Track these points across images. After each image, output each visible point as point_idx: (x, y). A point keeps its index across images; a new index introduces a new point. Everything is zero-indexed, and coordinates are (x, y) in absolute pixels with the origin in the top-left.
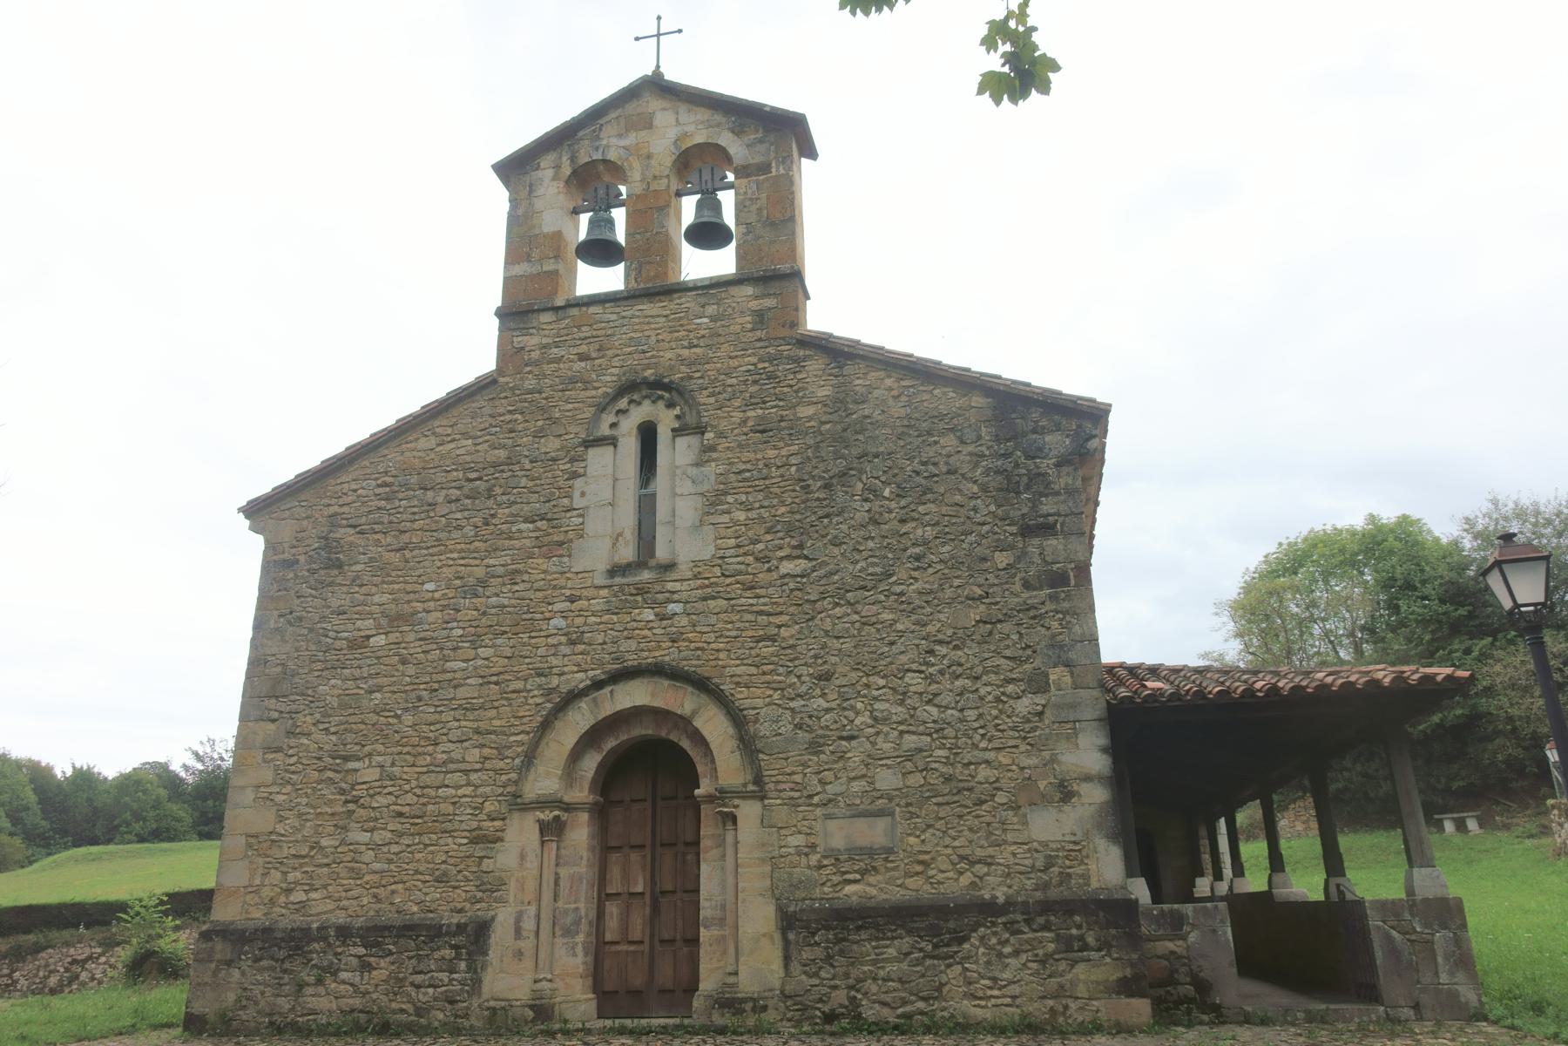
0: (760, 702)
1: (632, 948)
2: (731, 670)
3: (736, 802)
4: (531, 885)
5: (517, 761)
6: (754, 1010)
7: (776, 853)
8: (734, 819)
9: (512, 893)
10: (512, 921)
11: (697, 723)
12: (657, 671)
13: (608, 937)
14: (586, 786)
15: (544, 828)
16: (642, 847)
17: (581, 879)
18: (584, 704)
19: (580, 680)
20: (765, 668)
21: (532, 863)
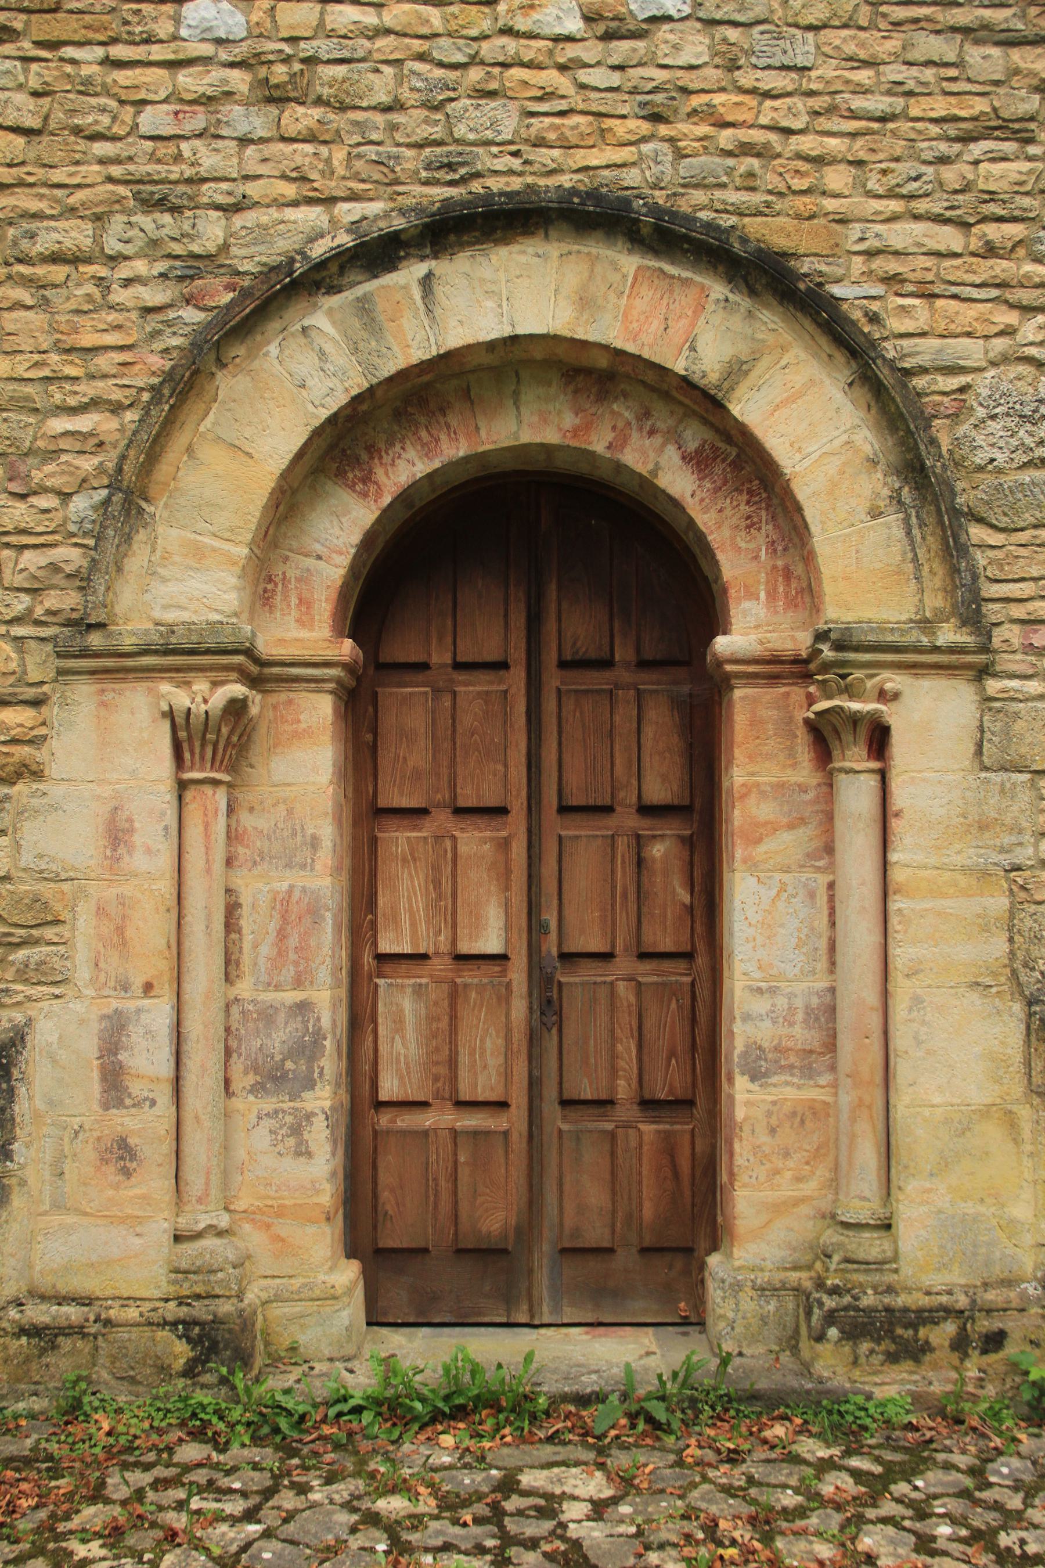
0: (972, 351)
1: (471, 1121)
2: (862, 235)
3: (893, 680)
4: (151, 930)
5: (81, 505)
6: (960, 1344)
7: (1025, 855)
8: (879, 738)
9: (82, 956)
10: (89, 1045)
11: (747, 408)
12: (597, 216)
13: (389, 1087)
14: (324, 606)
15: (187, 738)
16: (502, 811)
17: (314, 912)
18: (324, 318)
19: (316, 230)
20: (992, 231)
21: (150, 857)
